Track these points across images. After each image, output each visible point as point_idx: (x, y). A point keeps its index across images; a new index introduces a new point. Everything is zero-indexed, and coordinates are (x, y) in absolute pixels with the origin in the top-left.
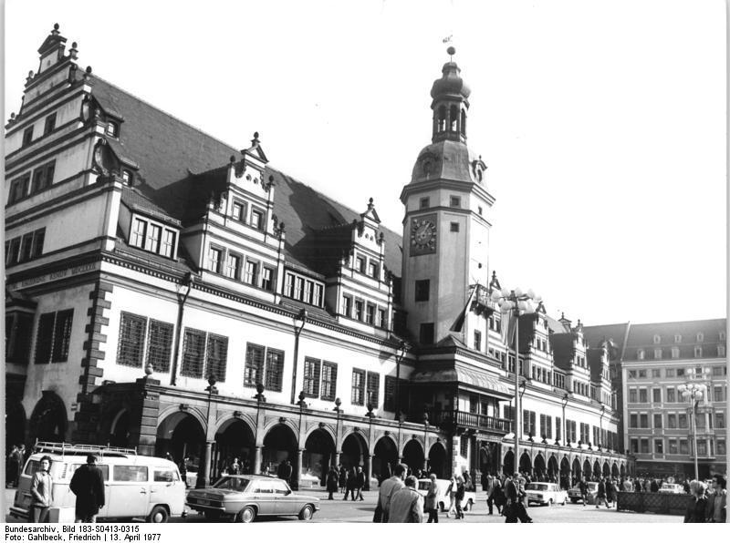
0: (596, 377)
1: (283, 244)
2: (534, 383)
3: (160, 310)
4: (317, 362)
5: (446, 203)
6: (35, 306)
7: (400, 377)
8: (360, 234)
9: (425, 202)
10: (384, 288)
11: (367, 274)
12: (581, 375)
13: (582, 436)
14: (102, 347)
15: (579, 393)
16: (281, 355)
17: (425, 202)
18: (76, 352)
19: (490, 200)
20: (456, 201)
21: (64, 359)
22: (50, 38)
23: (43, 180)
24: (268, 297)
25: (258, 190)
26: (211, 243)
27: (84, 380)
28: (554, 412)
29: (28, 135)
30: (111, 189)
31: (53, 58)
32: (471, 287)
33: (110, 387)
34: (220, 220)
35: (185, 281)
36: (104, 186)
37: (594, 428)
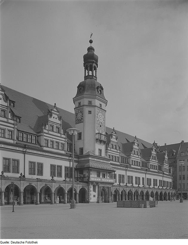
4: (34, 163)
8: (51, 116)
9: (80, 103)
10: (63, 136)
11: (55, 131)
12: (154, 162)
13: (160, 184)
15: (153, 169)
16: (18, 161)
20: (90, 102)
24: (11, 141)
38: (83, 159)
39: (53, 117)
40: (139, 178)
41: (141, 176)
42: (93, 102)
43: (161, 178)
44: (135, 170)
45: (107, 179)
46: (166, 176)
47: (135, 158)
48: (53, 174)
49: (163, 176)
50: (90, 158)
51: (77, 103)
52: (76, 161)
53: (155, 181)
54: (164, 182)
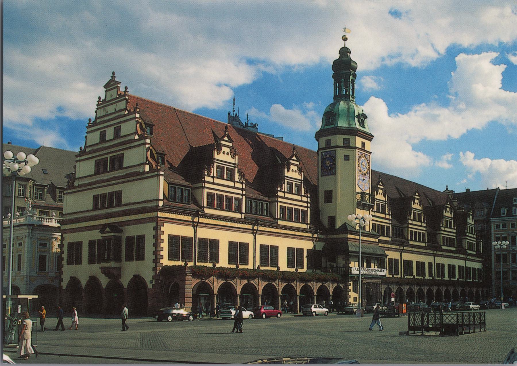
0: (461, 232)
1: (244, 185)
2: (411, 243)
3: (187, 231)
6: (121, 231)
7: (316, 249)
9: (328, 142)
10: (304, 199)
12: (448, 232)
14: (162, 253)
17: (328, 142)
19: (369, 137)
21: (143, 258)
22: (110, 81)
23: (117, 164)
24: (238, 216)
25: (229, 158)
26: (207, 192)
27: (154, 269)
28: (427, 259)
29: (103, 136)
30: (160, 175)
32: (358, 193)
33: (166, 269)
36: (154, 173)
37: (459, 266)
38: (336, 236)
39: (291, 169)
40: (423, 264)
41: (427, 259)
42: (352, 141)
43: (462, 263)
44: (416, 250)
45: (374, 270)
46: (471, 258)
47: (416, 226)
49: (465, 259)
50: (349, 236)
51: (323, 140)
52: (320, 240)
53: (451, 268)
54: (468, 269)
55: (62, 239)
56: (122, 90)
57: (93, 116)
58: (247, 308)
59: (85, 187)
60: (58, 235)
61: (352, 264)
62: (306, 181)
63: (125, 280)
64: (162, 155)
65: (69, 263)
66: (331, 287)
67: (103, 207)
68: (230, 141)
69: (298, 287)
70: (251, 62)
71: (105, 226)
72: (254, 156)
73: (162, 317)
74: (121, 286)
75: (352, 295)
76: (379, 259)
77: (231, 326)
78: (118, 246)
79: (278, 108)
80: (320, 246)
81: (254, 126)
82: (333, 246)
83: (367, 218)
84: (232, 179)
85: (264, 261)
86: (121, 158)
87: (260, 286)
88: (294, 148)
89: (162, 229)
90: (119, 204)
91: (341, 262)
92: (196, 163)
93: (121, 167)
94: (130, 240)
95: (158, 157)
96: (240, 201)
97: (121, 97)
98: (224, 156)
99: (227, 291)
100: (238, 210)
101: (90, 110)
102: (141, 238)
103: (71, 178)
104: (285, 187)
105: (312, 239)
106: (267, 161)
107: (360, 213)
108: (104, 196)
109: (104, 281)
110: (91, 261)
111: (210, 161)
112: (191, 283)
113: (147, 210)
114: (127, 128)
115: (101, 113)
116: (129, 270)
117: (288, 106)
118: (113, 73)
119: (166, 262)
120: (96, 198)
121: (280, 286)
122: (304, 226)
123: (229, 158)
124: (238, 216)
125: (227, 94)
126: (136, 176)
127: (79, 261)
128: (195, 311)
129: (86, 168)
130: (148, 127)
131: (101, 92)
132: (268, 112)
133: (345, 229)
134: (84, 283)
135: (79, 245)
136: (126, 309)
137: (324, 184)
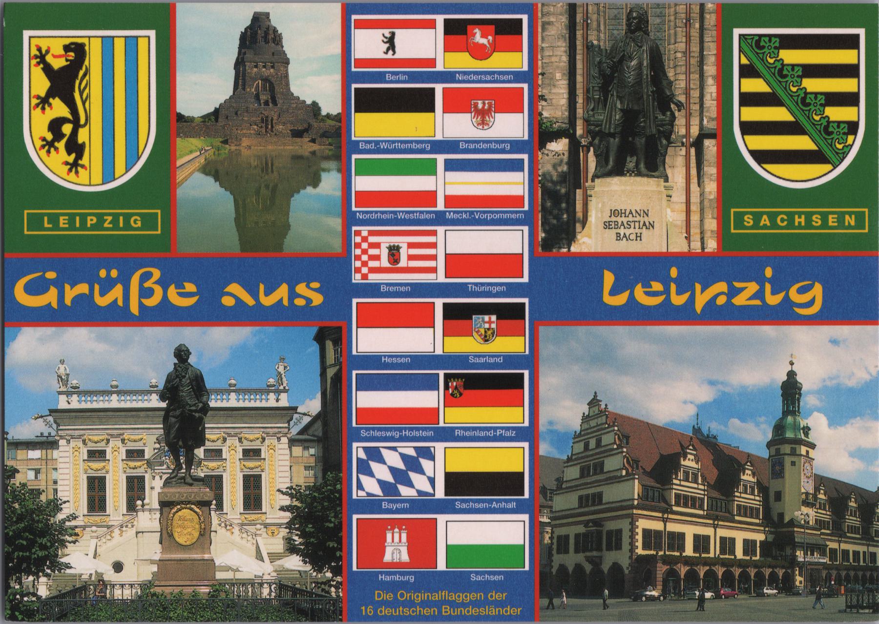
3: (658, 526)
5: (788, 451)
6: (602, 526)
10: (757, 498)
18: (626, 546)
21: (620, 548)
22: (593, 399)
24: (701, 512)
25: (693, 464)
27: (631, 558)
30: (635, 478)
31: (596, 409)
33: (641, 558)
34: (677, 482)
35: (663, 512)
36: (630, 477)
45: (817, 558)
48: (745, 553)
52: (771, 533)
55: (552, 532)
56: (603, 407)
57: (578, 429)
58: (708, 590)
59: (571, 489)
60: (549, 529)
61: (798, 553)
62: (759, 483)
63: (606, 567)
64: (636, 462)
65: (558, 552)
66: (781, 573)
67: (587, 506)
68: (695, 449)
69: (752, 572)
70: (712, 383)
71: (588, 521)
72: (716, 463)
73: (637, 598)
74: (603, 572)
75: (798, 579)
76: (821, 549)
77: (694, 605)
78: (599, 538)
79: (736, 422)
80: (771, 538)
81: (715, 437)
82: (781, 538)
83: (810, 514)
84: (696, 482)
85: (723, 551)
86: (602, 464)
87: (720, 571)
88: (749, 455)
89: (637, 523)
90: (600, 502)
91: (788, 551)
92: (665, 469)
93: (602, 471)
94: (610, 533)
95: (634, 463)
96: (702, 500)
97: (603, 413)
98: (689, 462)
99: (692, 576)
100: (701, 508)
101: (576, 424)
102: (619, 532)
103: (560, 481)
104: (741, 488)
105: (764, 532)
106: (726, 467)
107: (805, 510)
108: (587, 496)
109: (588, 568)
110: (577, 551)
111: (678, 466)
112: (661, 569)
113: (624, 508)
114: (607, 439)
115: (586, 426)
116: (609, 558)
117: (743, 419)
118: (596, 393)
119: (640, 551)
120: (581, 498)
121: (737, 572)
122: (757, 521)
123: (693, 464)
124: (701, 512)
125: (692, 410)
126: (614, 479)
127: (567, 552)
128: (665, 593)
129: (573, 473)
130: (625, 438)
131: (585, 409)
132: (726, 426)
133: (792, 523)
134: (571, 569)
135: (567, 537)
136: (606, 591)
137: (774, 486)
